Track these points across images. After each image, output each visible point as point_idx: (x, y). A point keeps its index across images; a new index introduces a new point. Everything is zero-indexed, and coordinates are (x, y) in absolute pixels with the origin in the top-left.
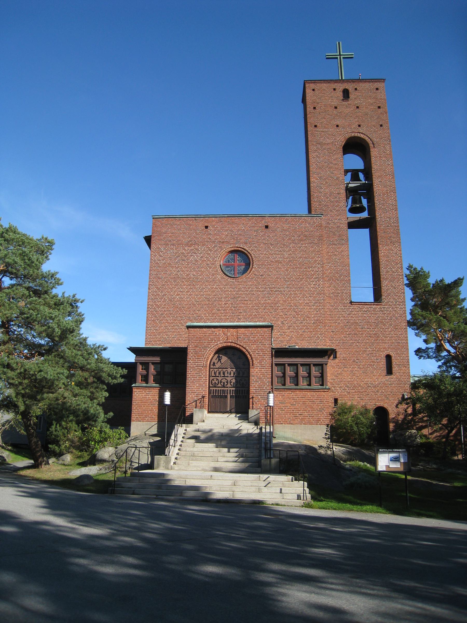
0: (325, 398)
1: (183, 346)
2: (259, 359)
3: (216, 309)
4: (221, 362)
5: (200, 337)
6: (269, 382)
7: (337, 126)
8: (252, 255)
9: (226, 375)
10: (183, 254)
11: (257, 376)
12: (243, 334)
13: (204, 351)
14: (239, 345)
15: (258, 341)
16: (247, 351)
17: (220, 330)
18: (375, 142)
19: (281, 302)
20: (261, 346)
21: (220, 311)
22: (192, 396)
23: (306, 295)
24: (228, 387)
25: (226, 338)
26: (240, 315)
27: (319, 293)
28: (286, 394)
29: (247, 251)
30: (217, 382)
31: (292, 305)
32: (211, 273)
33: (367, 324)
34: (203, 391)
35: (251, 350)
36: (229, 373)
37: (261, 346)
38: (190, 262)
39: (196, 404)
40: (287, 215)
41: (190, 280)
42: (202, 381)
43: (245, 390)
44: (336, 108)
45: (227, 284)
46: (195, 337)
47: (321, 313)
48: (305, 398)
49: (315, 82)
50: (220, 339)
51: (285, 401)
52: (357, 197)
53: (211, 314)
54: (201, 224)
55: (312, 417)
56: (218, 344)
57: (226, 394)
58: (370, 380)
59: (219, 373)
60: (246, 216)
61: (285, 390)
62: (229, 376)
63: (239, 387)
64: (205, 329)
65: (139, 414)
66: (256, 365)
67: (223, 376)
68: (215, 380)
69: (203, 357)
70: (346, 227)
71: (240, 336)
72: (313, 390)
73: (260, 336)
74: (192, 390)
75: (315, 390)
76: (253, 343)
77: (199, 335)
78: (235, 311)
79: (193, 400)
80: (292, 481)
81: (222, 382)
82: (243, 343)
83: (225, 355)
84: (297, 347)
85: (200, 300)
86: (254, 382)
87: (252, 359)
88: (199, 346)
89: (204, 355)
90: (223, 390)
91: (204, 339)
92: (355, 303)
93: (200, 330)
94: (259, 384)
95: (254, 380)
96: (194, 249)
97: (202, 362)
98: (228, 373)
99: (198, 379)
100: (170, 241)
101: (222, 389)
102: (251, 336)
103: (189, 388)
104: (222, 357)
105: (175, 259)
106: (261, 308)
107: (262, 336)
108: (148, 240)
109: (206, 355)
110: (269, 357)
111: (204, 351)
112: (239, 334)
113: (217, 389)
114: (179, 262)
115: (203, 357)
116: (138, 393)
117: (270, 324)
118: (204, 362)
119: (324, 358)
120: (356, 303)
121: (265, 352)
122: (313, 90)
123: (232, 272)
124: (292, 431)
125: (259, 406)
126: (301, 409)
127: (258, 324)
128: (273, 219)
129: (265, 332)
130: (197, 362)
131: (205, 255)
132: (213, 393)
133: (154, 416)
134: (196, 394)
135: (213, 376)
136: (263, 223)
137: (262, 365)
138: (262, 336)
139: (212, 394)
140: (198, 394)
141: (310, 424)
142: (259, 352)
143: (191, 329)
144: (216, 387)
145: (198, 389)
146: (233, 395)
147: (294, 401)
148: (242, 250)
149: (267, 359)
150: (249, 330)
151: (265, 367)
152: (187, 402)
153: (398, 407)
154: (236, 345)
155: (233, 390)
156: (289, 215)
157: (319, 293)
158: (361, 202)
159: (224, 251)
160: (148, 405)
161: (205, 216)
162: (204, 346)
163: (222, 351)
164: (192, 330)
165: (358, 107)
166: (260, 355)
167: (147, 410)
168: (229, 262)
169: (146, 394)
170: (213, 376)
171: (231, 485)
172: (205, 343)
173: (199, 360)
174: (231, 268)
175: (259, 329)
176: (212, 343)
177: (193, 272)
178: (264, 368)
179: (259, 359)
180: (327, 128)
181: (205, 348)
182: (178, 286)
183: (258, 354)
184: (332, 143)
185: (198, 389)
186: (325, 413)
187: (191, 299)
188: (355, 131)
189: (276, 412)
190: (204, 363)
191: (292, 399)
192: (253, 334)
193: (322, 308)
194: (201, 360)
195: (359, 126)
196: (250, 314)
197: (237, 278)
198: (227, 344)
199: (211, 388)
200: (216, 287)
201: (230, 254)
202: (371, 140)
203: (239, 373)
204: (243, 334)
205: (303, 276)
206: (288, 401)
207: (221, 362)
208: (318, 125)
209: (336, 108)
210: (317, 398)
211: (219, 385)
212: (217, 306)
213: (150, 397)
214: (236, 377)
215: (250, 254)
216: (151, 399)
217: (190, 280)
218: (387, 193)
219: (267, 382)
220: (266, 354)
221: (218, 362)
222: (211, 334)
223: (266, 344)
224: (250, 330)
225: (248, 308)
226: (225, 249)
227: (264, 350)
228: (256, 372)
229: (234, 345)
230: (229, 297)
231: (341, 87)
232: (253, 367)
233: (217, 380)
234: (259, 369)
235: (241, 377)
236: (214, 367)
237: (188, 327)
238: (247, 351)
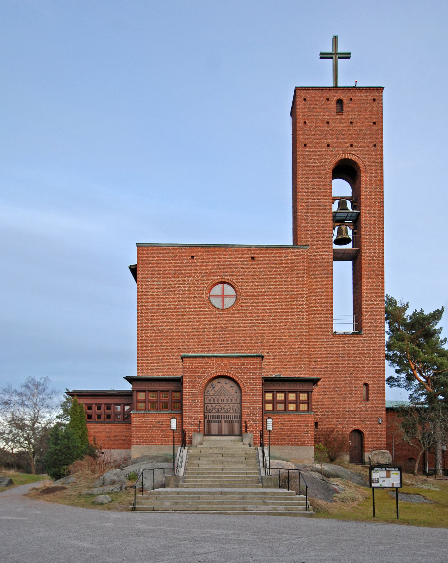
1: (179, 375)
2: (251, 387)
6: (260, 408)
9: (220, 401)
12: (236, 364)
13: (199, 380)
15: (249, 371)
17: (214, 361)
22: (189, 421)
24: (221, 413)
33: (347, 355)
35: (243, 379)
36: (223, 400)
42: (198, 408)
45: (215, 316)
50: (214, 369)
55: (299, 439)
65: (138, 438)
67: (217, 402)
69: (198, 385)
82: (236, 372)
86: (246, 408)
94: (251, 410)
95: (246, 406)
97: (197, 391)
98: (221, 400)
99: (194, 406)
102: (243, 366)
105: (163, 290)
107: (253, 366)
108: (134, 270)
109: (201, 384)
110: (260, 386)
111: (199, 380)
113: (212, 414)
114: (167, 293)
115: (198, 385)
116: (137, 419)
118: (199, 390)
124: (280, 451)
126: (289, 432)
127: (249, 355)
130: (193, 390)
132: (208, 418)
133: (153, 439)
137: (253, 392)
138: (253, 366)
139: (207, 419)
141: (296, 445)
142: (251, 381)
144: (211, 413)
145: (194, 415)
149: (258, 387)
151: (256, 394)
160: (147, 429)
162: (199, 375)
166: (251, 384)
167: (146, 434)
169: (145, 419)
176: (206, 372)
178: (255, 396)
179: (251, 387)
181: (200, 377)
183: (249, 382)
186: (310, 435)
189: (266, 435)
190: (199, 391)
191: (280, 423)
192: (245, 364)
194: (196, 389)
195: (352, 146)
197: (225, 310)
199: (206, 414)
204: (236, 364)
210: (303, 422)
211: (214, 411)
213: (148, 423)
216: (149, 425)
219: (258, 408)
220: (258, 382)
223: (257, 374)
227: (255, 379)
228: (248, 399)
234: (251, 396)
236: (209, 394)
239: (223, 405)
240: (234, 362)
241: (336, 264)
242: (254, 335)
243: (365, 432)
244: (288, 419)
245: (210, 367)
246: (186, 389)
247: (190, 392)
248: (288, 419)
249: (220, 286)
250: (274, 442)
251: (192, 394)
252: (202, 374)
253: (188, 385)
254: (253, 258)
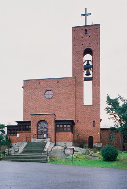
52: (88, 70)
54: (38, 83)
58: (88, 128)
84: (66, 119)
122: (75, 31)
136: (57, 81)
158: (89, 72)
181: (36, 121)
208: (76, 44)
209: (82, 37)
237: (31, 115)
239: (43, 129)
241: (85, 82)
242: (58, 106)
243: (94, 137)
249: (48, 91)
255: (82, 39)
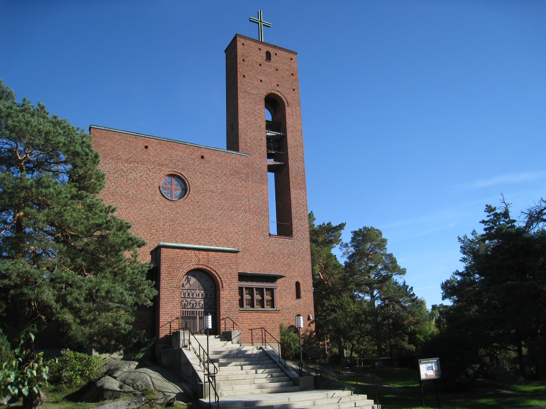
0: (276, 319)
2: (228, 282)
3: (155, 230)
4: (189, 284)
5: (173, 258)
6: (237, 304)
7: (261, 81)
8: (189, 181)
9: (195, 296)
10: (123, 170)
11: (226, 298)
12: (214, 257)
14: (210, 268)
15: (226, 265)
16: (217, 273)
18: (288, 102)
19: (215, 229)
20: (229, 270)
21: (159, 231)
23: (235, 225)
24: (197, 309)
25: (197, 260)
26: (177, 238)
27: (246, 224)
28: (244, 315)
29: (185, 177)
30: (186, 303)
31: (224, 233)
32: (150, 193)
34: (177, 312)
35: (221, 273)
37: (229, 270)
38: (129, 179)
39: (170, 326)
40: (221, 150)
41: (129, 197)
42: (175, 302)
43: (185, 311)
44: (260, 65)
46: (167, 257)
47: (248, 242)
48: (260, 319)
49: (245, 38)
50: (192, 261)
51: (244, 322)
53: (149, 233)
54: (141, 144)
56: (190, 266)
57: (195, 316)
59: (189, 295)
60: (185, 144)
61: (244, 312)
62: (198, 297)
63: (208, 309)
64: (177, 250)
66: (225, 287)
67: (192, 297)
68: (184, 301)
69: (176, 278)
70: (266, 169)
71: (211, 259)
72: (266, 312)
73: (228, 260)
74: (166, 312)
75: (268, 312)
76: (223, 266)
77: (172, 256)
78: (172, 233)
79: (167, 321)
80: (352, 395)
81: (191, 303)
83: (194, 276)
85: (138, 219)
87: (221, 282)
88: (172, 267)
89: (177, 276)
90: (192, 311)
91: (177, 260)
92: (273, 236)
93: (172, 251)
96: (133, 167)
98: (196, 295)
99: (171, 300)
100: (109, 155)
101: (192, 310)
103: (163, 310)
104: (190, 278)
106: (197, 233)
112: (210, 257)
113: (187, 310)
117: (237, 249)
119: (274, 283)
120: (274, 236)
121: (233, 275)
123: (169, 195)
125: (229, 327)
128: (208, 151)
129: (233, 257)
130: (170, 283)
131: (145, 174)
134: (170, 316)
135: (182, 298)
136: (199, 153)
140: (172, 316)
143: (164, 249)
144: (185, 308)
145: (172, 310)
146: (201, 316)
147: (251, 322)
148: (180, 175)
149: (235, 282)
150: (218, 254)
152: (161, 324)
153: (310, 326)
154: (206, 268)
155: (201, 312)
156: (222, 150)
157: (246, 224)
159: (163, 173)
161: (146, 136)
162: (177, 267)
163: (194, 272)
164: (164, 250)
165: (277, 70)
166: (228, 279)
168: (166, 185)
170: (182, 298)
171: (312, 405)
172: (178, 263)
173: (173, 281)
174: (168, 190)
175: (227, 254)
176: (184, 264)
177: (131, 189)
179: (228, 282)
180: (253, 80)
182: (116, 202)
183: (227, 277)
184: (257, 94)
185: (172, 310)
187: (129, 216)
188: (274, 89)
193: (248, 238)
196: (186, 238)
198: (198, 266)
200: (155, 208)
201: (168, 177)
202: (286, 99)
203: (206, 295)
204: (214, 257)
205: (233, 207)
206: (247, 322)
207: (189, 284)
208: (246, 76)
211: (189, 306)
212: (155, 227)
214: (204, 298)
215: (187, 180)
217: (129, 197)
218: (297, 146)
220: (234, 277)
221: (187, 283)
222: (183, 255)
224: (219, 254)
225: (185, 232)
226: (163, 172)
227: (232, 274)
229: (204, 267)
230: (167, 219)
231: (265, 49)
232: (222, 289)
233: (186, 301)
235: (209, 299)
238: (217, 273)
240: (212, 255)
244: (256, 315)
245: (188, 259)
246: (163, 282)
247: (167, 285)
248: (256, 315)
250: (244, 339)
251: (169, 287)
252: (180, 265)
253: (165, 277)
254: (202, 157)
255: (260, 68)
